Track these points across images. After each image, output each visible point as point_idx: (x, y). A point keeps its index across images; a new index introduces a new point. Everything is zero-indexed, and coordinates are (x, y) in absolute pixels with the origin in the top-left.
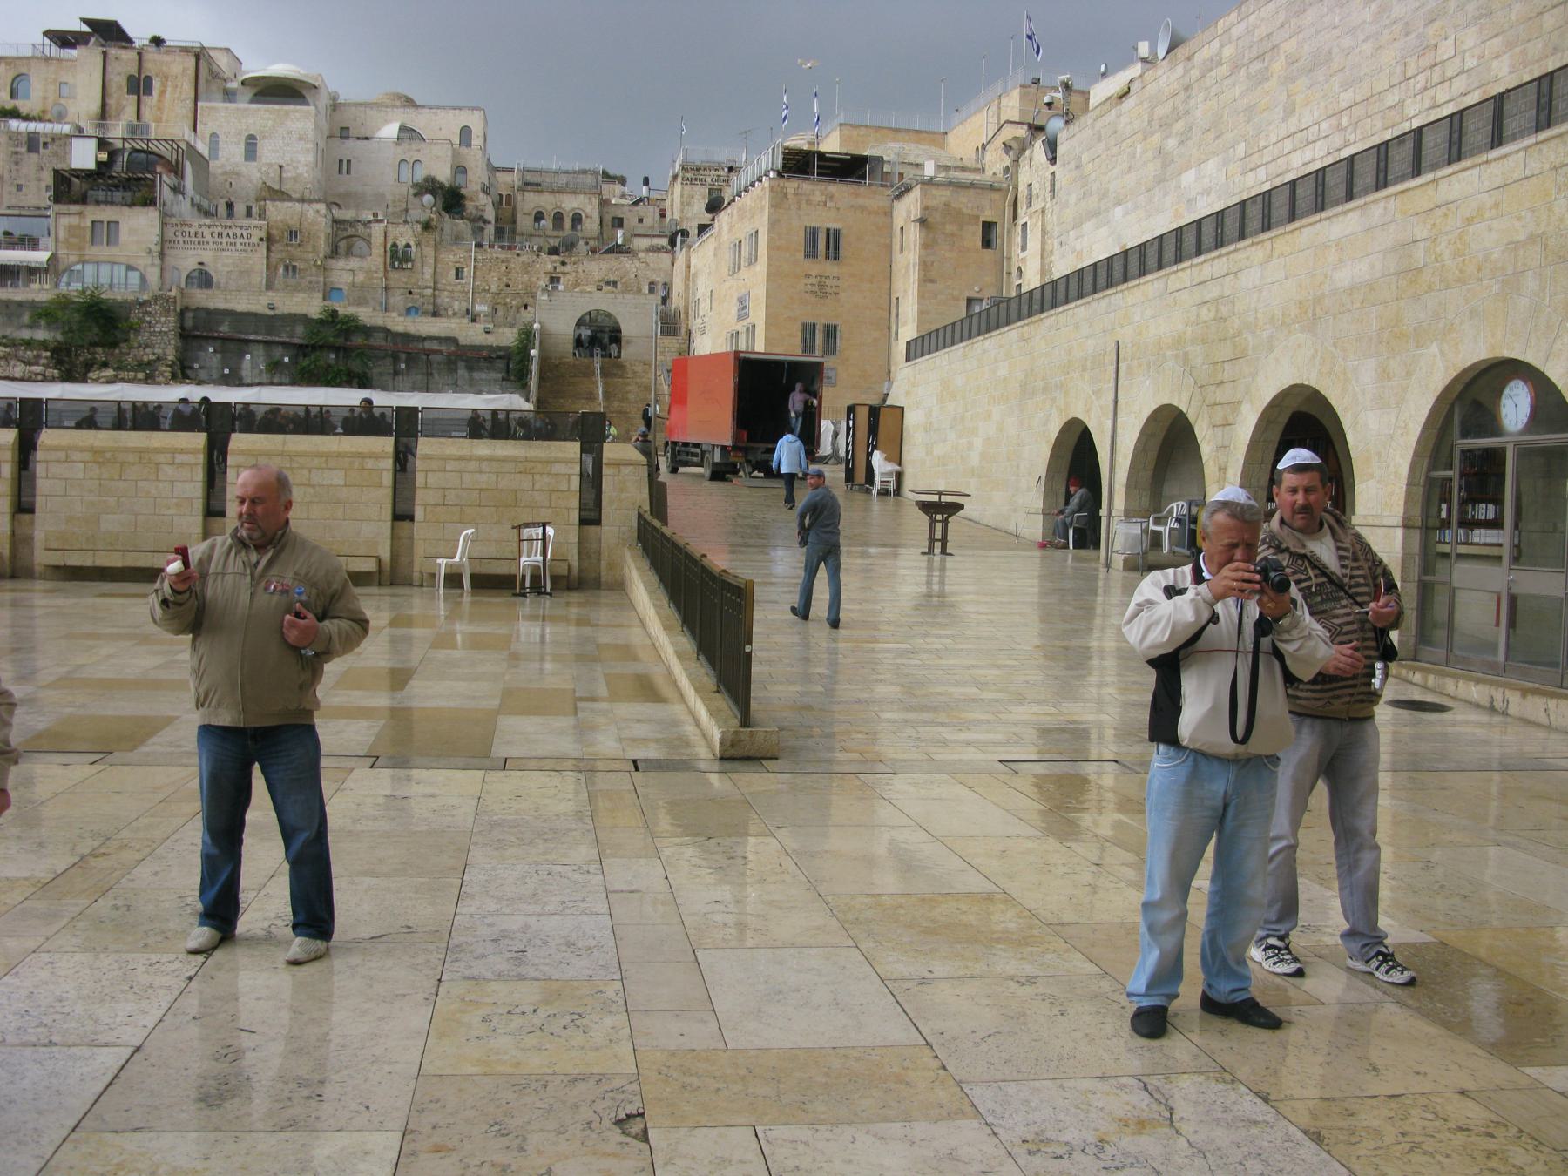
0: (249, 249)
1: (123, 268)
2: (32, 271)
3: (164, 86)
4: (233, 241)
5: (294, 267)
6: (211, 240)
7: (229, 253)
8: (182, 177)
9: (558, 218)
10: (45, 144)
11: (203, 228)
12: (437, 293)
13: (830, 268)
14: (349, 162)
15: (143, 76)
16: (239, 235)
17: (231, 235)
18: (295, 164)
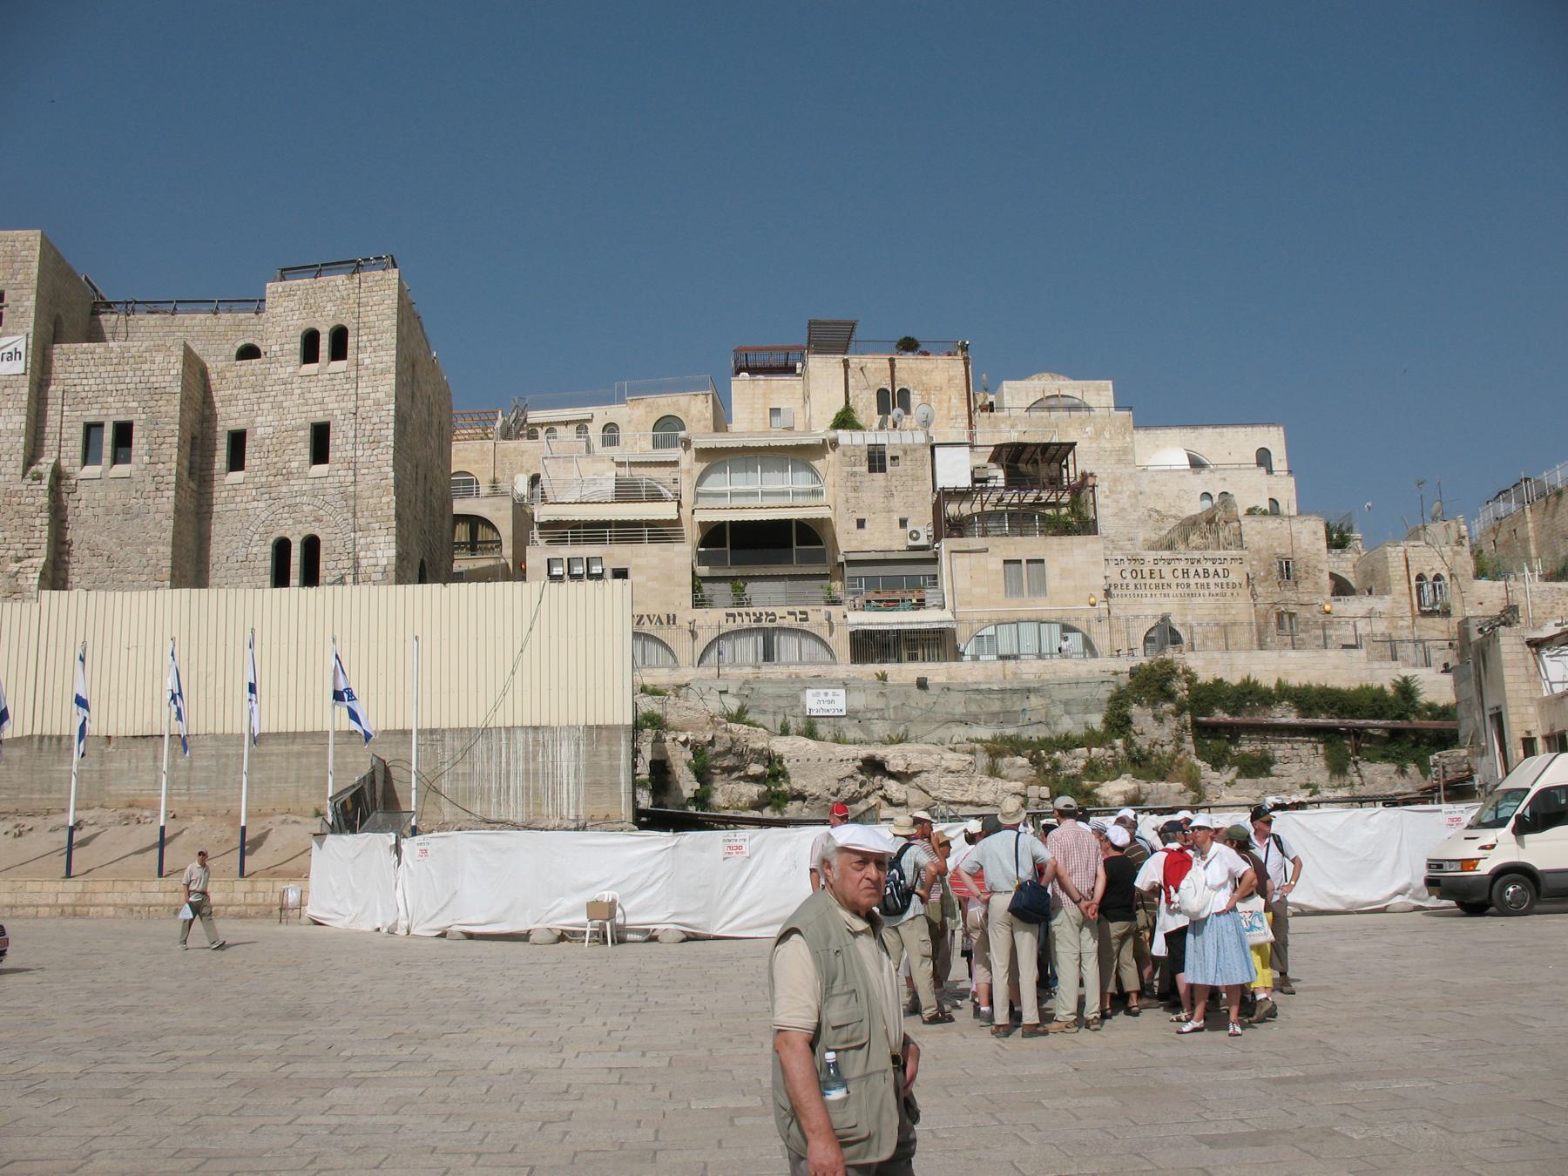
0: (1229, 592)
1: (1056, 629)
5: (1292, 615)
7: (1200, 600)
15: (897, 390)
16: (1212, 571)
17: (1201, 572)
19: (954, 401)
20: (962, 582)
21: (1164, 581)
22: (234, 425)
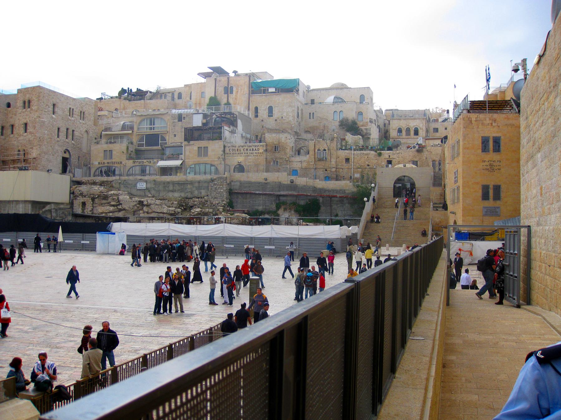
0: (259, 155)
2: (177, 169)
3: (237, 89)
4: (252, 152)
5: (277, 162)
6: (243, 152)
7: (250, 157)
8: (236, 127)
9: (408, 130)
10: (184, 118)
11: (240, 147)
12: (337, 170)
13: (495, 157)
14: (313, 113)
15: (229, 87)
16: (254, 149)
18: (288, 117)
19: (245, 89)
20: (187, 153)
21: (241, 152)
22: (12, 123)
